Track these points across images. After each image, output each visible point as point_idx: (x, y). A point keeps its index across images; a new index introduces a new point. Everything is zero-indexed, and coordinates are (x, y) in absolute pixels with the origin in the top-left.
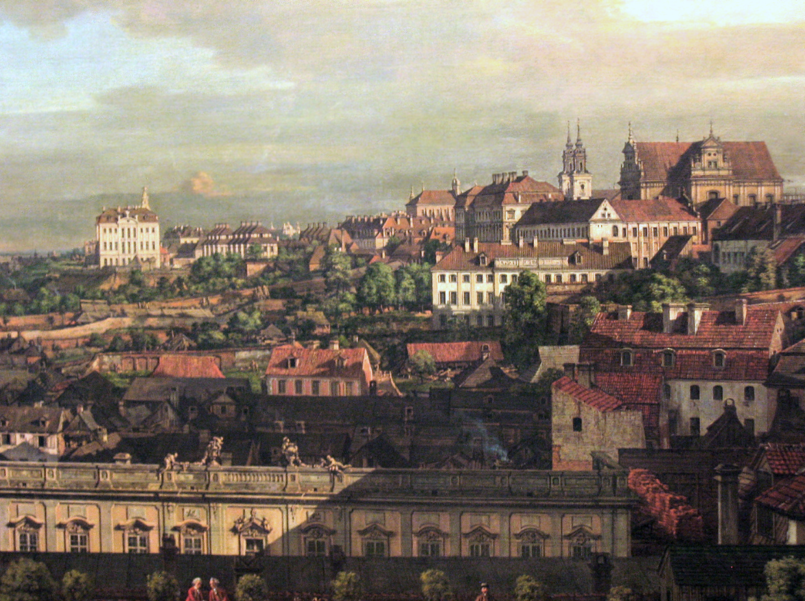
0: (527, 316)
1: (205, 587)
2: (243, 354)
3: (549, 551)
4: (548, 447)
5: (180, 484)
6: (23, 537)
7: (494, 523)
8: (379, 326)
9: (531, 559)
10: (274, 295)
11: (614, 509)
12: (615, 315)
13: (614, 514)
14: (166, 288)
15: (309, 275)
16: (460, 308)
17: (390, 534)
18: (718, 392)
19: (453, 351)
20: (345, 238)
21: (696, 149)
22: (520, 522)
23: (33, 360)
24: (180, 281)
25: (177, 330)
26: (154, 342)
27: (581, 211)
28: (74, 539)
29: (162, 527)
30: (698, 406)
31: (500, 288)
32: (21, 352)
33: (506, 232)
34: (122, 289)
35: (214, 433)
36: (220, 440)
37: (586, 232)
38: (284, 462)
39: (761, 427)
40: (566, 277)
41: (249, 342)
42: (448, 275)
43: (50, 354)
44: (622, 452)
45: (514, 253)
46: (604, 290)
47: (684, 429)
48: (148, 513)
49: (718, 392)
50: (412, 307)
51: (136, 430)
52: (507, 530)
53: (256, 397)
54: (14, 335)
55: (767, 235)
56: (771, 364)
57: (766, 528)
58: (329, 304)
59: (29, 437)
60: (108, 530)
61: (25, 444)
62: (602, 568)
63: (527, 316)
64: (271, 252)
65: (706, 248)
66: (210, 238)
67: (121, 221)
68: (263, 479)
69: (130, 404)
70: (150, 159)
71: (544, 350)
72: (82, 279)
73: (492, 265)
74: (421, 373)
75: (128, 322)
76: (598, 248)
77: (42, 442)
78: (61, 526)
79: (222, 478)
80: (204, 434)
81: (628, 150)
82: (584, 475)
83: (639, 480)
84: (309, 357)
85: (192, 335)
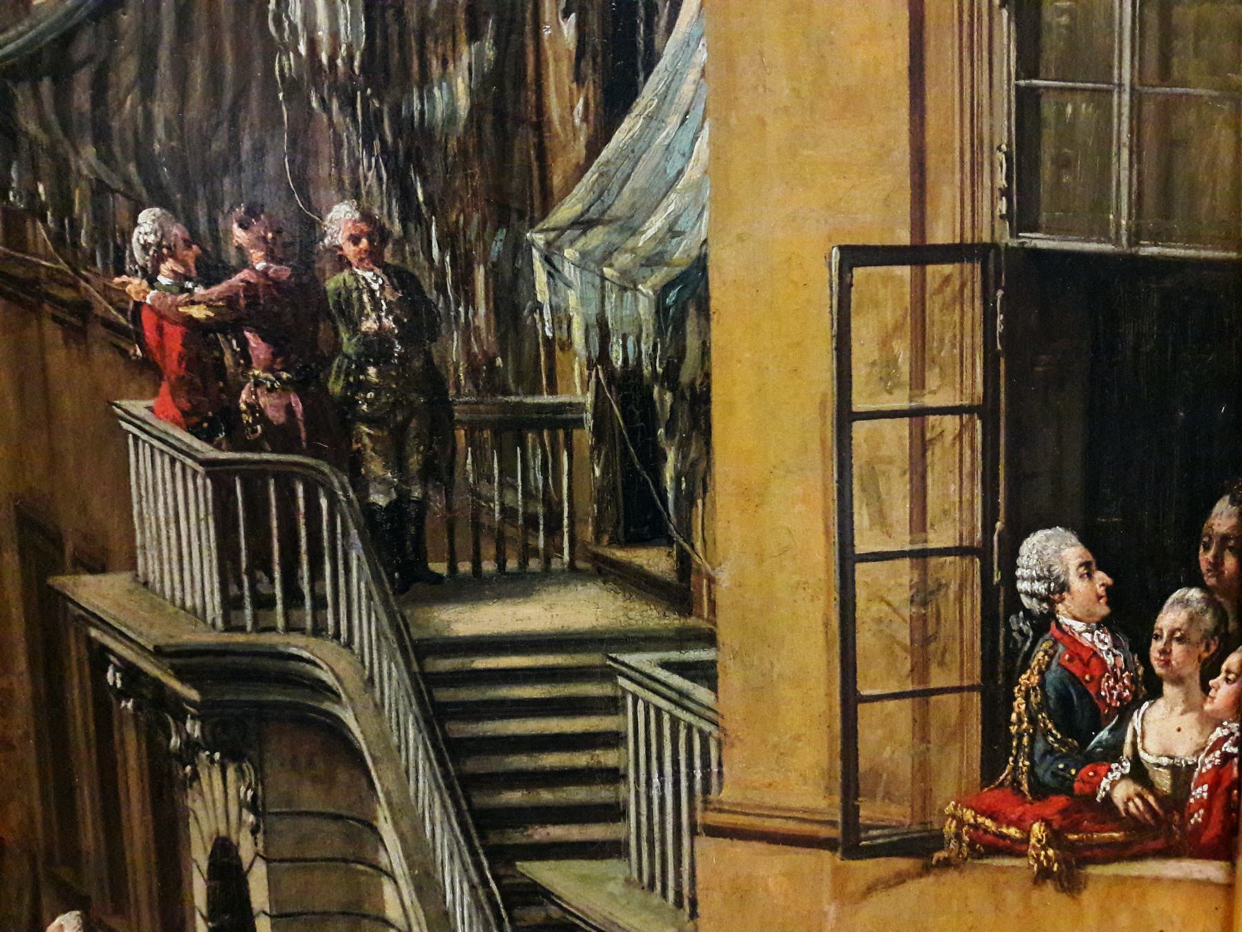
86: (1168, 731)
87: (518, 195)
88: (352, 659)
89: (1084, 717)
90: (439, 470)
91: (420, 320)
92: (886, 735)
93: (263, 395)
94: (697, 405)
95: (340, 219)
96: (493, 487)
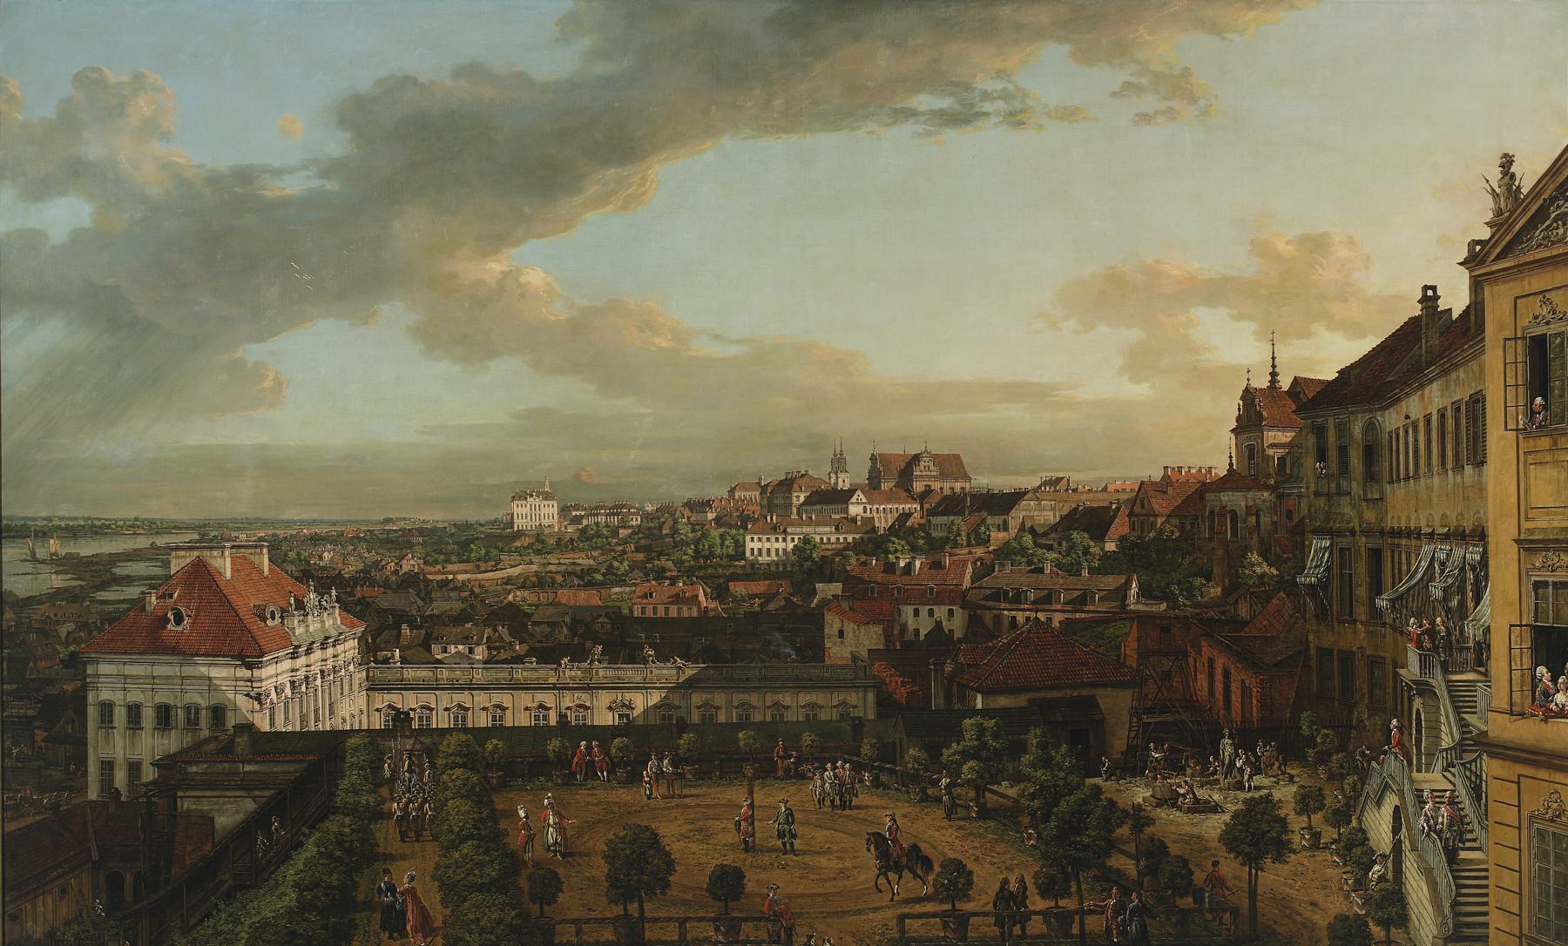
0: (808, 564)
1: (589, 747)
2: (616, 590)
3: (823, 717)
4: (823, 649)
6: (456, 718)
7: (787, 699)
9: (811, 722)
10: (637, 550)
11: (865, 688)
12: (864, 564)
14: (562, 544)
15: (662, 537)
16: (764, 559)
17: (718, 708)
19: (760, 587)
20: (687, 512)
21: (916, 458)
22: (805, 698)
24: (572, 540)
25: (570, 574)
27: (844, 497)
30: (918, 621)
31: (791, 546)
32: (455, 588)
34: (530, 546)
35: (596, 643)
37: (846, 510)
38: (645, 662)
39: (958, 634)
40: (833, 539)
41: (620, 582)
43: (477, 590)
45: (799, 523)
46: (856, 547)
47: (910, 636)
48: (548, 698)
50: (732, 558)
52: (795, 704)
55: (961, 513)
56: (964, 594)
57: (962, 699)
58: (676, 556)
60: (519, 710)
62: (858, 726)
63: (808, 564)
64: (636, 521)
66: (593, 511)
68: (630, 673)
69: (535, 624)
71: (819, 586)
72: (502, 538)
73: (785, 531)
74: (739, 601)
75: (534, 568)
76: (854, 520)
77: (471, 651)
79: (601, 673)
80: (589, 644)
81: (873, 458)
82: (843, 667)
83: (878, 667)
84: (663, 591)
85: (580, 577)
86: (1560, 698)
87: (1463, 617)
88: (1437, 682)
89: (1547, 695)
90: (1451, 655)
91: (1449, 633)
92: (1517, 697)
93: (1427, 644)
96: (1459, 658)
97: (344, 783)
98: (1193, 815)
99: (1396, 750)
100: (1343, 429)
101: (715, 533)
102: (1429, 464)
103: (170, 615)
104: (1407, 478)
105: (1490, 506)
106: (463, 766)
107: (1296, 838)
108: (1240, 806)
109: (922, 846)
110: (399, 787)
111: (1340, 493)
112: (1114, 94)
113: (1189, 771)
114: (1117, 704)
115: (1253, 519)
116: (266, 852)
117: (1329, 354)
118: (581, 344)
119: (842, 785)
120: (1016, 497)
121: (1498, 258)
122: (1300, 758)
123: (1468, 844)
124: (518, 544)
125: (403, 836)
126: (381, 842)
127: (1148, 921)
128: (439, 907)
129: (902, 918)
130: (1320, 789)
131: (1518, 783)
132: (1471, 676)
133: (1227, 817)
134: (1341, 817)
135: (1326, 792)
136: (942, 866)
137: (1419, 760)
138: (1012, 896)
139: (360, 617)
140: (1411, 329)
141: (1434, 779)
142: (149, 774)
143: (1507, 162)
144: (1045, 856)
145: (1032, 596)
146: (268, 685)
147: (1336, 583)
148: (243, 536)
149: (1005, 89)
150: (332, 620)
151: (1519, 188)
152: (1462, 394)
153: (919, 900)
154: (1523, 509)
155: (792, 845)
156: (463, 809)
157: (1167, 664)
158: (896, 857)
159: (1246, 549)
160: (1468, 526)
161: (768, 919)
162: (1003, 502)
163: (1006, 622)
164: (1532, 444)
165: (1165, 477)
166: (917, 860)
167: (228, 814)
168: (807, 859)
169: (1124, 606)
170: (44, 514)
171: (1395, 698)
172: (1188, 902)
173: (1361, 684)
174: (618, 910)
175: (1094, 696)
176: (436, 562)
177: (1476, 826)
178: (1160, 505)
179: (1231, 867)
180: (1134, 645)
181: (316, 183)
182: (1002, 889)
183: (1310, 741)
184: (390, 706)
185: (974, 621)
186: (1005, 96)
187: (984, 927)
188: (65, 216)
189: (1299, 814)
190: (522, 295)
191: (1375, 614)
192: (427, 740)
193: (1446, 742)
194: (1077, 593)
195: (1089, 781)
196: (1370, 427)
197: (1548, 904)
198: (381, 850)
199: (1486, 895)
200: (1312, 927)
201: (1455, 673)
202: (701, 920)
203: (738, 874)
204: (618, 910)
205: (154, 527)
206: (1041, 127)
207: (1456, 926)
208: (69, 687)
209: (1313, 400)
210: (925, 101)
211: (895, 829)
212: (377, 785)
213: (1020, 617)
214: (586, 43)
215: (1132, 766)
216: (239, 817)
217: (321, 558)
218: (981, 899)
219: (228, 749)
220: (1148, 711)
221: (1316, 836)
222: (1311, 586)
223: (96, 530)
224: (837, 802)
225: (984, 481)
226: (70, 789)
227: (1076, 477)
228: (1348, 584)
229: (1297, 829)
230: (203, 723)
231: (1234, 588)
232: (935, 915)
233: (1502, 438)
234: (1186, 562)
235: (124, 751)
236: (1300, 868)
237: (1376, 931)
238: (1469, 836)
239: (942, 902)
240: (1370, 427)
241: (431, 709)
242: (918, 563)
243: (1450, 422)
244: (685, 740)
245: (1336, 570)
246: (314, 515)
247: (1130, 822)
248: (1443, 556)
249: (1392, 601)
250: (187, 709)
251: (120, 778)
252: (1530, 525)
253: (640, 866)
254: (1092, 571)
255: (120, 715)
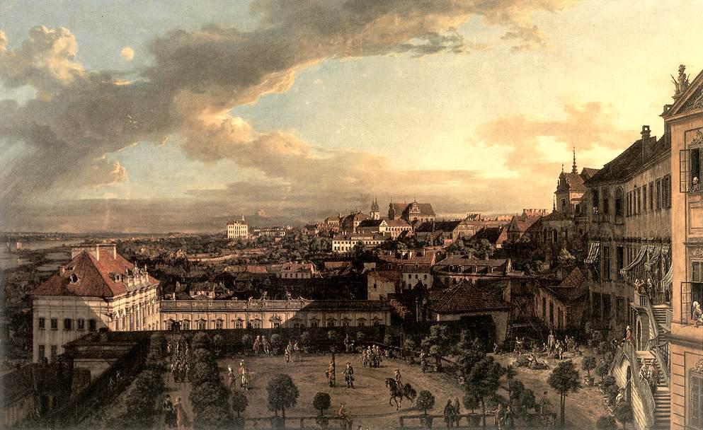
1: (261, 339)
3: (366, 324)
4: (367, 292)
5: (254, 306)
6: (200, 325)
7: (350, 316)
8: (316, 257)
9: (361, 327)
10: (284, 247)
11: (386, 312)
12: (386, 254)
13: (386, 313)
14: (249, 245)
15: (295, 242)
16: (341, 252)
17: (319, 320)
18: (417, 277)
20: (306, 230)
21: (411, 205)
22: (358, 316)
23: (205, 268)
25: (253, 258)
26: (246, 262)
28: (218, 325)
29: (247, 320)
30: (411, 281)
31: (353, 246)
32: (201, 265)
33: (355, 229)
34: (235, 245)
36: (266, 293)
40: (372, 243)
42: (337, 242)
43: (211, 266)
44: (388, 294)
45: (357, 235)
46: (382, 246)
47: (407, 288)
48: (243, 316)
49: (417, 277)
51: (239, 290)
52: (354, 318)
53: (278, 279)
54: (198, 260)
57: (430, 317)
58: (301, 250)
59: (203, 292)
61: (202, 295)
62: (382, 329)
64: (283, 234)
65: (413, 234)
67: (235, 224)
68: (280, 304)
69: (237, 282)
70: (245, 206)
72: (222, 243)
75: (237, 256)
76: (382, 234)
77: (208, 294)
78: (213, 321)
79: (267, 304)
81: (391, 205)
82: (378, 301)
83: (394, 303)
84: (295, 266)
85: (258, 260)
88: (648, 309)
90: (654, 296)
94: (672, 292)
95: (649, 280)
97: (150, 355)
98: (534, 369)
99: (629, 340)
100: (605, 192)
101: (319, 240)
102: (645, 208)
103: (71, 278)
104: (635, 214)
105: (673, 227)
106: (203, 347)
107: (583, 381)
108: (557, 366)
109: (411, 385)
110: (174, 357)
111: (604, 221)
112: (502, 38)
113: (534, 350)
114: (501, 320)
115: (564, 233)
116: (114, 387)
117: (599, 157)
118: (255, 154)
119: (375, 356)
120: (457, 223)
121: (677, 113)
122: (585, 344)
123: (661, 384)
124: (229, 245)
125: (176, 379)
126: (166, 382)
127: (515, 420)
128: (192, 413)
129: (402, 418)
130: (594, 358)
131: (685, 356)
132: (663, 306)
133: (551, 371)
134: (604, 371)
135: (597, 360)
136: (421, 394)
137: (639, 345)
138: (453, 408)
139: (157, 278)
140: (635, 149)
141: (646, 354)
142: (61, 351)
143: (682, 69)
144: (468, 389)
145: (463, 269)
146: (116, 310)
147: (602, 263)
148: (105, 241)
149: (453, 36)
150: (145, 280)
151: (687, 81)
152: (661, 175)
153: (410, 410)
154: (688, 228)
155: (352, 383)
156: (203, 368)
157: (524, 300)
158: (400, 390)
159: (560, 248)
160: (663, 236)
161: (341, 418)
162: (450, 226)
163: (451, 282)
164: (691, 199)
165: (524, 214)
166: (409, 391)
167: (98, 369)
168: (359, 390)
169: (504, 274)
170: (14, 231)
171: (629, 317)
172: (532, 411)
173: (613, 310)
174: (273, 414)
175: (490, 316)
176: (192, 253)
177: (665, 376)
178: (522, 227)
179: (553, 394)
180: (509, 291)
181: (139, 79)
182: (448, 405)
183: (589, 336)
184: (171, 320)
185: (436, 282)
186: (453, 39)
187: (439, 423)
188: (25, 94)
189: (584, 369)
190: (233, 131)
191: (620, 277)
192: (187, 335)
193: (652, 336)
194: (483, 268)
195: (488, 355)
196: (618, 191)
197: (697, 412)
198: (165, 386)
199: (670, 407)
200: (590, 422)
201: (655, 304)
202: (311, 418)
203: (327, 397)
204: (273, 414)
205: (65, 237)
206: (468, 53)
207: (657, 422)
208: (25, 311)
209: (594, 179)
210: (415, 42)
211: (399, 376)
212: (164, 356)
213: (457, 279)
214: (262, 15)
215: (507, 348)
216: (102, 371)
217: (140, 251)
218: (438, 410)
219: (97, 339)
220: (515, 322)
221: (592, 380)
222: (590, 264)
223: (39, 238)
224: (373, 364)
225: (442, 216)
226: (25, 358)
227: (483, 214)
228: (607, 264)
229: (583, 376)
230: (86, 327)
231: (555, 265)
232: (417, 417)
233: (679, 196)
234: (533, 253)
235: (50, 341)
236: (584, 395)
237: (619, 424)
238: (661, 380)
239: (420, 410)
240: (618, 191)
241: (189, 321)
242: (411, 254)
243: (655, 189)
244: (304, 335)
245: (602, 257)
246: (136, 231)
247: (507, 374)
248: (651, 251)
249: (628, 271)
250: (79, 321)
251: (48, 353)
252: (691, 236)
253: (283, 394)
254: (491, 257)
255: (48, 324)
